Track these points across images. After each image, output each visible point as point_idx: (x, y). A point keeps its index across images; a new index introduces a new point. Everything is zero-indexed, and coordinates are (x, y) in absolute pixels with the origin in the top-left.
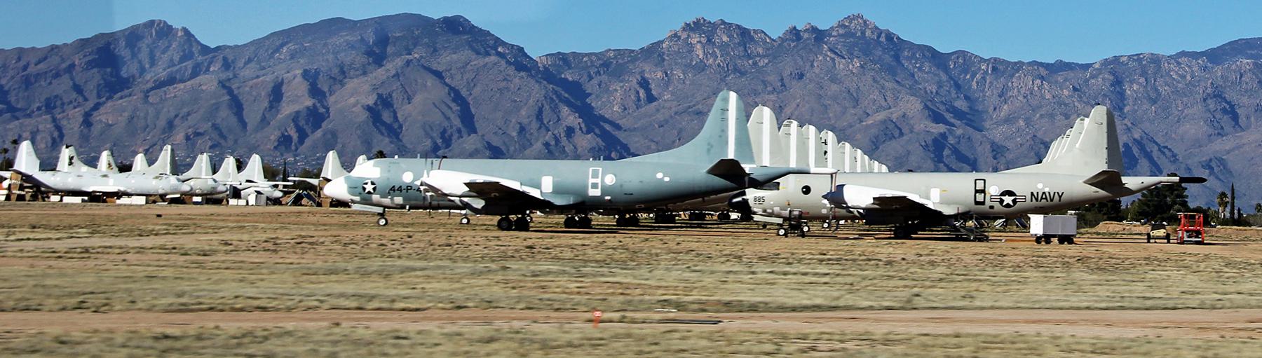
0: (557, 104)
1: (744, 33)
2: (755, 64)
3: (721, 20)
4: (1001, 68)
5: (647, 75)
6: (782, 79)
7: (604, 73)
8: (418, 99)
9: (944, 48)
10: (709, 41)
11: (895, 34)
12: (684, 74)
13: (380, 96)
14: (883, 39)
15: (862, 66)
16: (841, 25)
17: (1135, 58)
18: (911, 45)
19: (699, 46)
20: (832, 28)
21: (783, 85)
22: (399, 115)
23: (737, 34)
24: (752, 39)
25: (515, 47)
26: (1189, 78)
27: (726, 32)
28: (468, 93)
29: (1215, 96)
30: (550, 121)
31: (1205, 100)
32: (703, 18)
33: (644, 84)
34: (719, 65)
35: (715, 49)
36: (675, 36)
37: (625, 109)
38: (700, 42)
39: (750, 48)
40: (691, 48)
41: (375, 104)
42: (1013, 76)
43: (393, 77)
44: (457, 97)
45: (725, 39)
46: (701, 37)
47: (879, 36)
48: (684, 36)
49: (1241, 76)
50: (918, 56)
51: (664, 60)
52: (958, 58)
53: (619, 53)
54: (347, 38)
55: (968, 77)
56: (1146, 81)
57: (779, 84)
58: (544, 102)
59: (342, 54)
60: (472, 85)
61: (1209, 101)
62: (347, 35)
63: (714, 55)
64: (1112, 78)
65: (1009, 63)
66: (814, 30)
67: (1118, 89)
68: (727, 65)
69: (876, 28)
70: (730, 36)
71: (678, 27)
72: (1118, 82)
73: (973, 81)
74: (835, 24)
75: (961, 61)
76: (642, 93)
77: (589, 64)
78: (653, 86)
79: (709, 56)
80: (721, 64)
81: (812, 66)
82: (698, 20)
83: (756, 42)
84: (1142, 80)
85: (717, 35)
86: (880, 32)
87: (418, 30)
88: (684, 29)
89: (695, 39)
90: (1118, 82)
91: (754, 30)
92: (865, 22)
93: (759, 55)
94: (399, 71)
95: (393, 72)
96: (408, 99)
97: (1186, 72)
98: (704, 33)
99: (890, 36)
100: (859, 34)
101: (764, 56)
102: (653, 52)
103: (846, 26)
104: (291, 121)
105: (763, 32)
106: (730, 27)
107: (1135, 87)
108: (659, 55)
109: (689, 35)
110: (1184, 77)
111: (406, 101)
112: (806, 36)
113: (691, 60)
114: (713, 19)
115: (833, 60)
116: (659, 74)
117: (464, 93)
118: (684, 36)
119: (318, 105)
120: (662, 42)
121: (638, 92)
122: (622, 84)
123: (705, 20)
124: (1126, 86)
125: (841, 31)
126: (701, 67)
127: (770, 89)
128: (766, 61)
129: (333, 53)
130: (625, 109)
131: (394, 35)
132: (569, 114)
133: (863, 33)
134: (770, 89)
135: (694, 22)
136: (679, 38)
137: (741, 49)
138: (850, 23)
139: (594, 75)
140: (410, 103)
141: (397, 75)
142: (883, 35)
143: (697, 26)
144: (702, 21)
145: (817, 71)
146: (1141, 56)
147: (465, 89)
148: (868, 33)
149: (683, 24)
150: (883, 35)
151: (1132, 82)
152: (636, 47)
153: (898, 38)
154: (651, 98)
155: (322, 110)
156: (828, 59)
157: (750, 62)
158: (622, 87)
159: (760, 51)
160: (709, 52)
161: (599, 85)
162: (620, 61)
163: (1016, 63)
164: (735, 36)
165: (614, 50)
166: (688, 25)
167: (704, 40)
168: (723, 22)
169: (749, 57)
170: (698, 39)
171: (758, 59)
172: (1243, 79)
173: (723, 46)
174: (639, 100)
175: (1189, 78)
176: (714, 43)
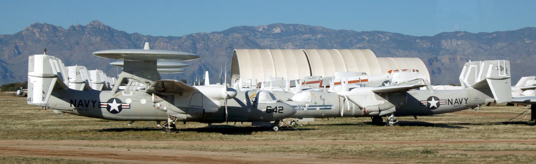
1: (54, 28)
2: (59, 39)
3: (45, 23)
4: (151, 39)
5: (17, 44)
6: (70, 45)
9: (129, 32)
10: (41, 31)
11: (111, 27)
14: (107, 29)
15: (101, 39)
16: (91, 24)
17: (198, 34)
18: (117, 31)
19: (37, 33)
20: (87, 25)
21: (71, 47)
24: (57, 30)
26: (220, 41)
29: (230, 47)
31: (226, 49)
33: (17, 47)
36: (27, 29)
37: (10, 57)
38: (37, 31)
40: (34, 33)
42: (155, 42)
45: (47, 30)
46: (37, 30)
47: (105, 28)
48: (31, 29)
49: (239, 40)
50: (120, 35)
51: (23, 38)
52: (135, 35)
53: (6, 36)
55: (139, 42)
56: (204, 42)
57: (69, 47)
61: (228, 49)
64: (192, 42)
65: (154, 37)
66: (80, 26)
67: (194, 46)
69: (104, 25)
71: (28, 25)
72: (194, 43)
73: (141, 44)
74: (88, 24)
75: (136, 36)
76: (16, 51)
78: (20, 48)
81: (82, 40)
82: (36, 23)
84: (203, 42)
86: (106, 27)
88: (31, 27)
89: (35, 30)
90: (194, 43)
92: (100, 23)
93: (61, 36)
97: (218, 39)
99: (109, 28)
100: (98, 27)
101: (62, 36)
102: (19, 36)
103: (92, 25)
105: (62, 27)
107: (200, 45)
109: (33, 29)
110: (218, 41)
112: (78, 28)
113: (35, 38)
114: (42, 22)
115: (89, 37)
116: (22, 44)
118: (31, 29)
120: (22, 32)
121: (14, 51)
122: (8, 48)
123: (38, 23)
124: (197, 45)
125: (91, 26)
126: (39, 41)
127: (66, 48)
128: (64, 38)
130: (10, 57)
133: (99, 27)
134: (66, 48)
135: (35, 24)
136: (29, 30)
138: (94, 23)
142: (107, 28)
143: (36, 26)
145: (83, 41)
146: (200, 34)
148: (101, 27)
149: (30, 25)
150: (107, 28)
151: (199, 43)
152: (12, 33)
153: (112, 29)
154: (19, 53)
156: (88, 37)
157: (58, 38)
158: (8, 49)
159: (61, 34)
162: (6, 39)
163: (156, 37)
164: (51, 29)
166: (32, 25)
167: (39, 31)
168: (46, 24)
169: (57, 37)
170: (37, 30)
171: (60, 37)
172: (239, 41)
174: (15, 53)
175: (220, 41)
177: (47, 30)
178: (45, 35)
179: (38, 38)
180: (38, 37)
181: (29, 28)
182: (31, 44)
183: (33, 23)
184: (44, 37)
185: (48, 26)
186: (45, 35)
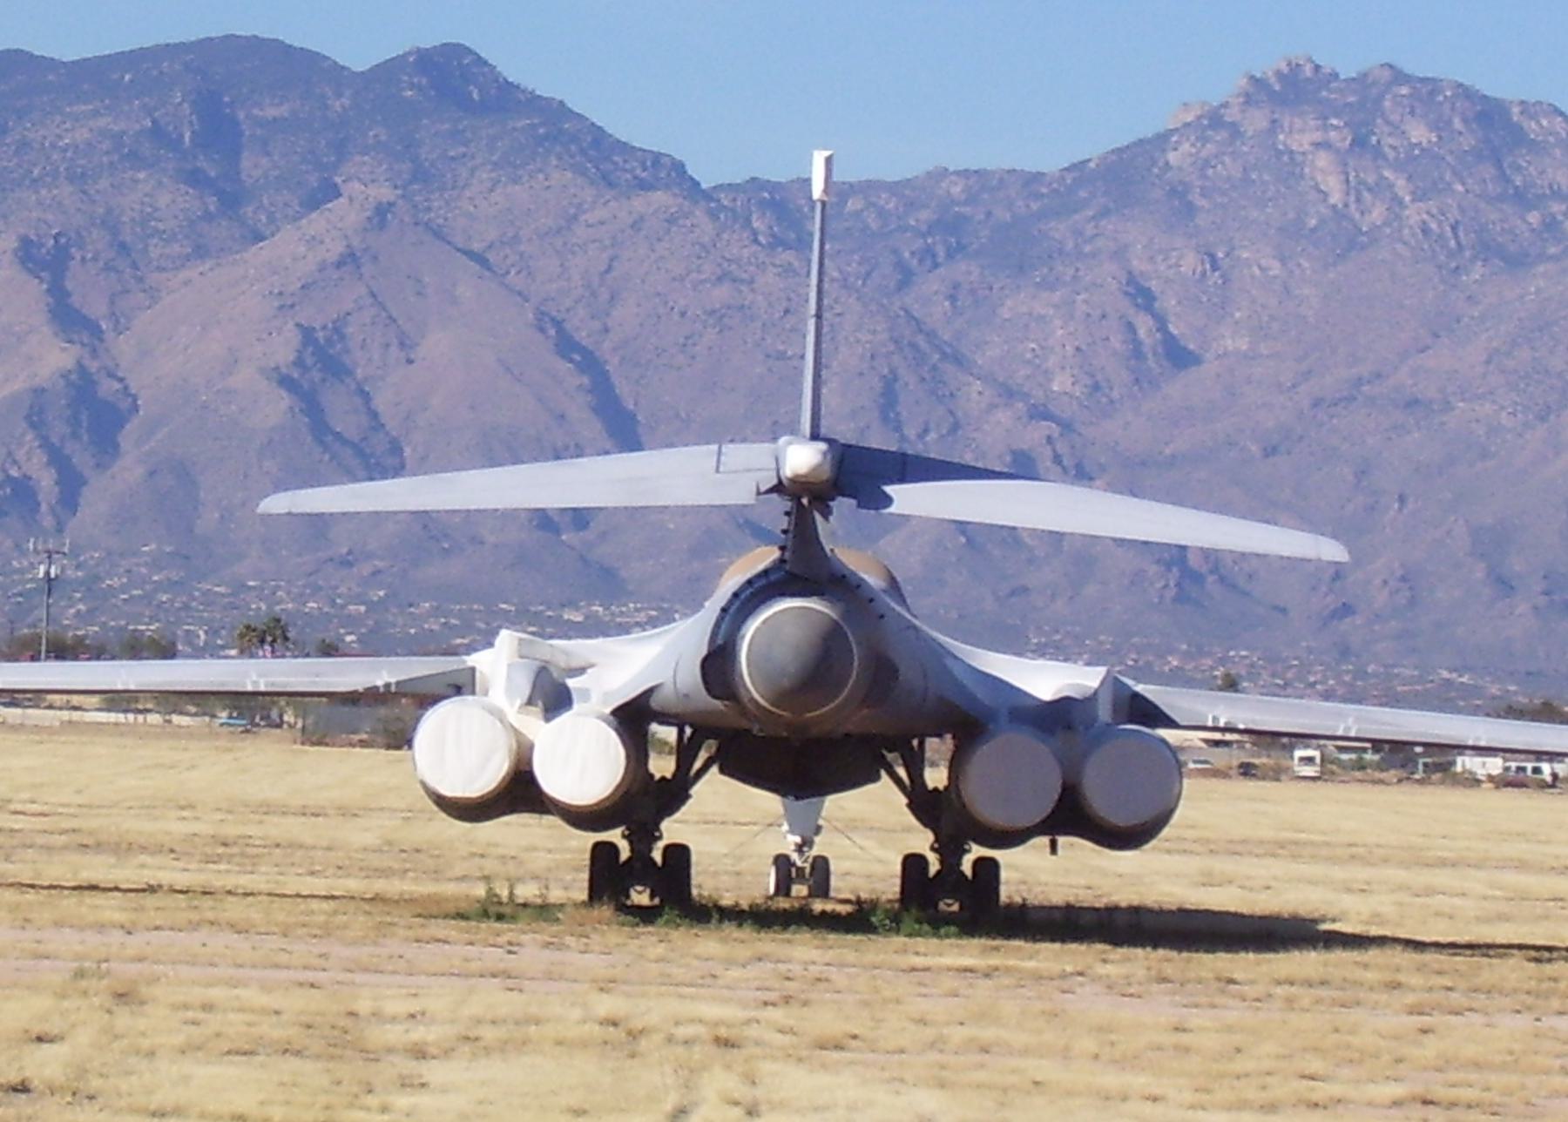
0: (934, 368)
3: (1391, 66)
7: (950, 255)
8: (437, 344)
10: (1359, 143)
12: (1283, 261)
13: (307, 333)
19: (1323, 160)
22: (381, 402)
23: (1465, 121)
24: (1518, 137)
25: (664, 160)
27: (1418, 111)
28: (597, 325)
30: (926, 431)
32: (1310, 60)
34: (1425, 231)
35: (1387, 173)
36: (1214, 119)
39: (1519, 169)
40: (1290, 168)
41: (299, 363)
43: (339, 265)
44: (566, 345)
45: (1419, 133)
48: (1256, 121)
54: (102, 122)
58: (896, 359)
59: (104, 184)
60: (604, 295)
62: (96, 113)
63: (1381, 188)
68: (1454, 228)
70: (1440, 126)
77: (873, 223)
78: (1168, 303)
79: (1366, 195)
80: (1434, 226)
82: (1295, 68)
83: (1535, 147)
85: (1388, 122)
87: (339, 96)
88: (1248, 100)
89: (1301, 135)
91: (1522, 102)
94: (356, 242)
95: (335, 249)
96: (402, 345)
98: (1337, 116)
104: (24, 425)
106: (1432, 93)
108: (1173, 192)
109: (1274, 121)
111: (394, 350)
117: (583, 331)
119: (93, 366)
121: (1131, 328)
123: (1317, 68)
129: (71, 179)
130: (1096, 387)
131: (256, 111)
132: (992, 407)
135: (1279, 74)
136: (1235, 131)
137: (1488, 171)
139: (915, 262)
140: (410, 362)
141: (349, 259)
144: (1308, 71)
147: (581, 312)
155: (108, 388)
157: (1534, 218)
160: (1361, 182)
161: (953, 298)
164: (1457, 124)
165: (965, 174)
168: (1399, 77)
169: (1522, 199)
170: (1318, 136)
173: (1410, 161)
176: (1378, 152)
177: (1419, 133)
178: (1401, 185)
179: (1339, 214)
180: (1336, 198)
181: (1232, 115)
182: (1276, 269)
183: (1268, 64)
184: (1401, 203)
185: (1426, 93)
186: (1401, 185)
